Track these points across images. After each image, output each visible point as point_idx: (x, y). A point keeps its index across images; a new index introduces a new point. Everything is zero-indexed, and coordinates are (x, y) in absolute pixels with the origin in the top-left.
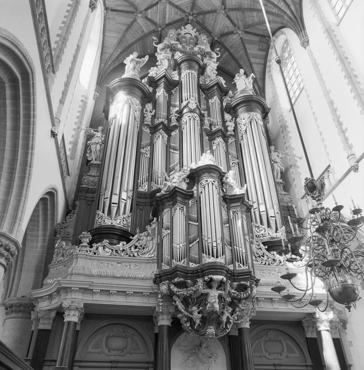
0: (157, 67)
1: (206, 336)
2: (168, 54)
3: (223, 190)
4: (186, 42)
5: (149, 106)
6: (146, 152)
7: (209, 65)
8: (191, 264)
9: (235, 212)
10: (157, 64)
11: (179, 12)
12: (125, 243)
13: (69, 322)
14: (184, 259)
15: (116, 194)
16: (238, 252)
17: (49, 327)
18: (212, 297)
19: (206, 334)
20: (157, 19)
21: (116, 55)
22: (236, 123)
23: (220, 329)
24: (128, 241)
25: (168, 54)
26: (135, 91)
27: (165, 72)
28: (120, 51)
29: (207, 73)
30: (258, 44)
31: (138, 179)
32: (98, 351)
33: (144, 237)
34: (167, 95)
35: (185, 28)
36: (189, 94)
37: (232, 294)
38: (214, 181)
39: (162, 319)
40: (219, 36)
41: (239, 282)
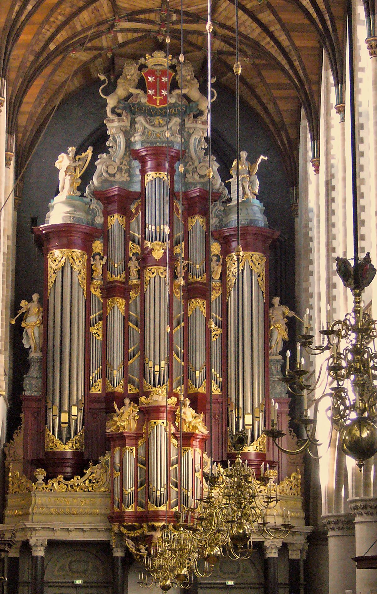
0: (108, 153)
3: (174, 425)
4: (153, 86)
5: (98, 246)
6: (98, 331)
7: (193, 132)
8: (138, 508)
10: (107, 144)
12: (79, 478)
13: (37, 557)
15: (65, 412)
17: (17, 555)
21: (39, 110)
22: (224, 265)
24: (82, 475)
25: (124, 121)
28: (44, 101)
29: (189, 152)
31: (90, 375)
32: (62, 573)
33: (98, 471)
34: (124, 219)
35: (152, 57)
36: (154, 227)
38: (163, 423)
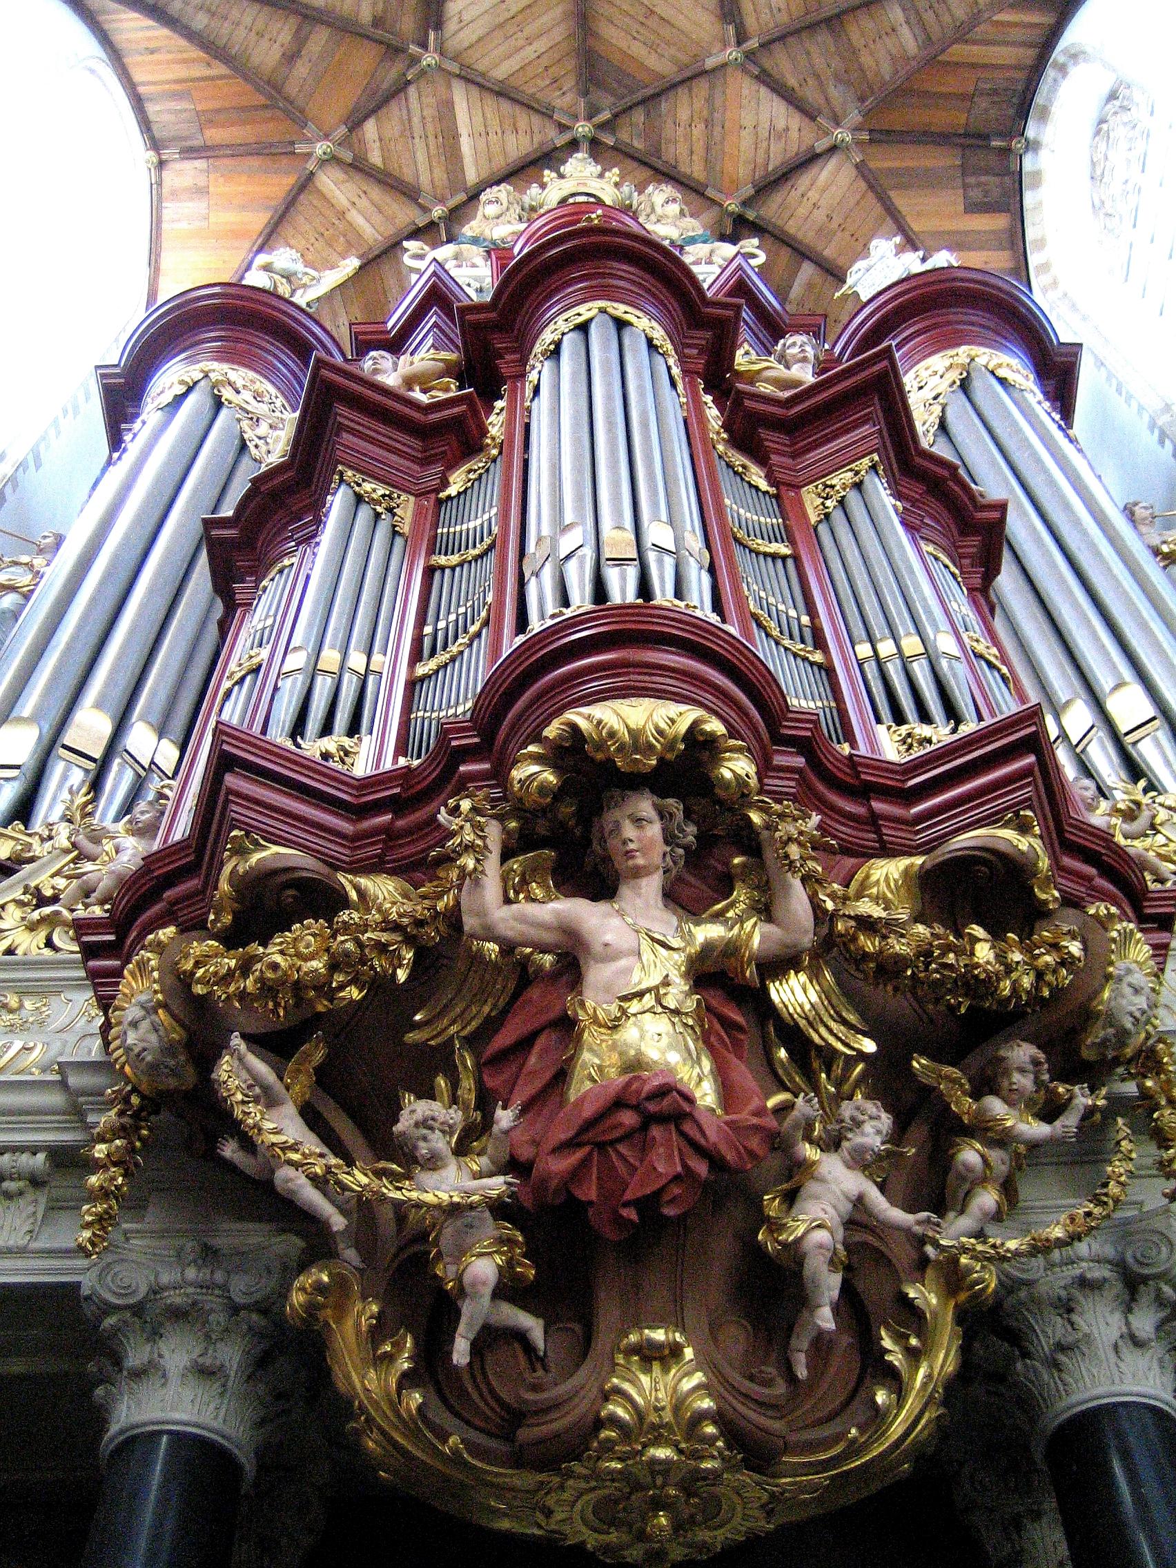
1: (607, 1448)
2: (474, 266)
9: (832, 487)
11: (523, 119)
14: (353, 729)
16: (894, 671)
18: (610, 954)
19: (599, 1424)
20: (423, 168)
23: (791, 1378)
25: (474, 266)
26: (262, 348)
27: (434, 274)
30: (960, 181)
35: (561, 176)
37: (869, 944)
39: (138, 1374)
40: (748, 191)
41: (926, 848)
